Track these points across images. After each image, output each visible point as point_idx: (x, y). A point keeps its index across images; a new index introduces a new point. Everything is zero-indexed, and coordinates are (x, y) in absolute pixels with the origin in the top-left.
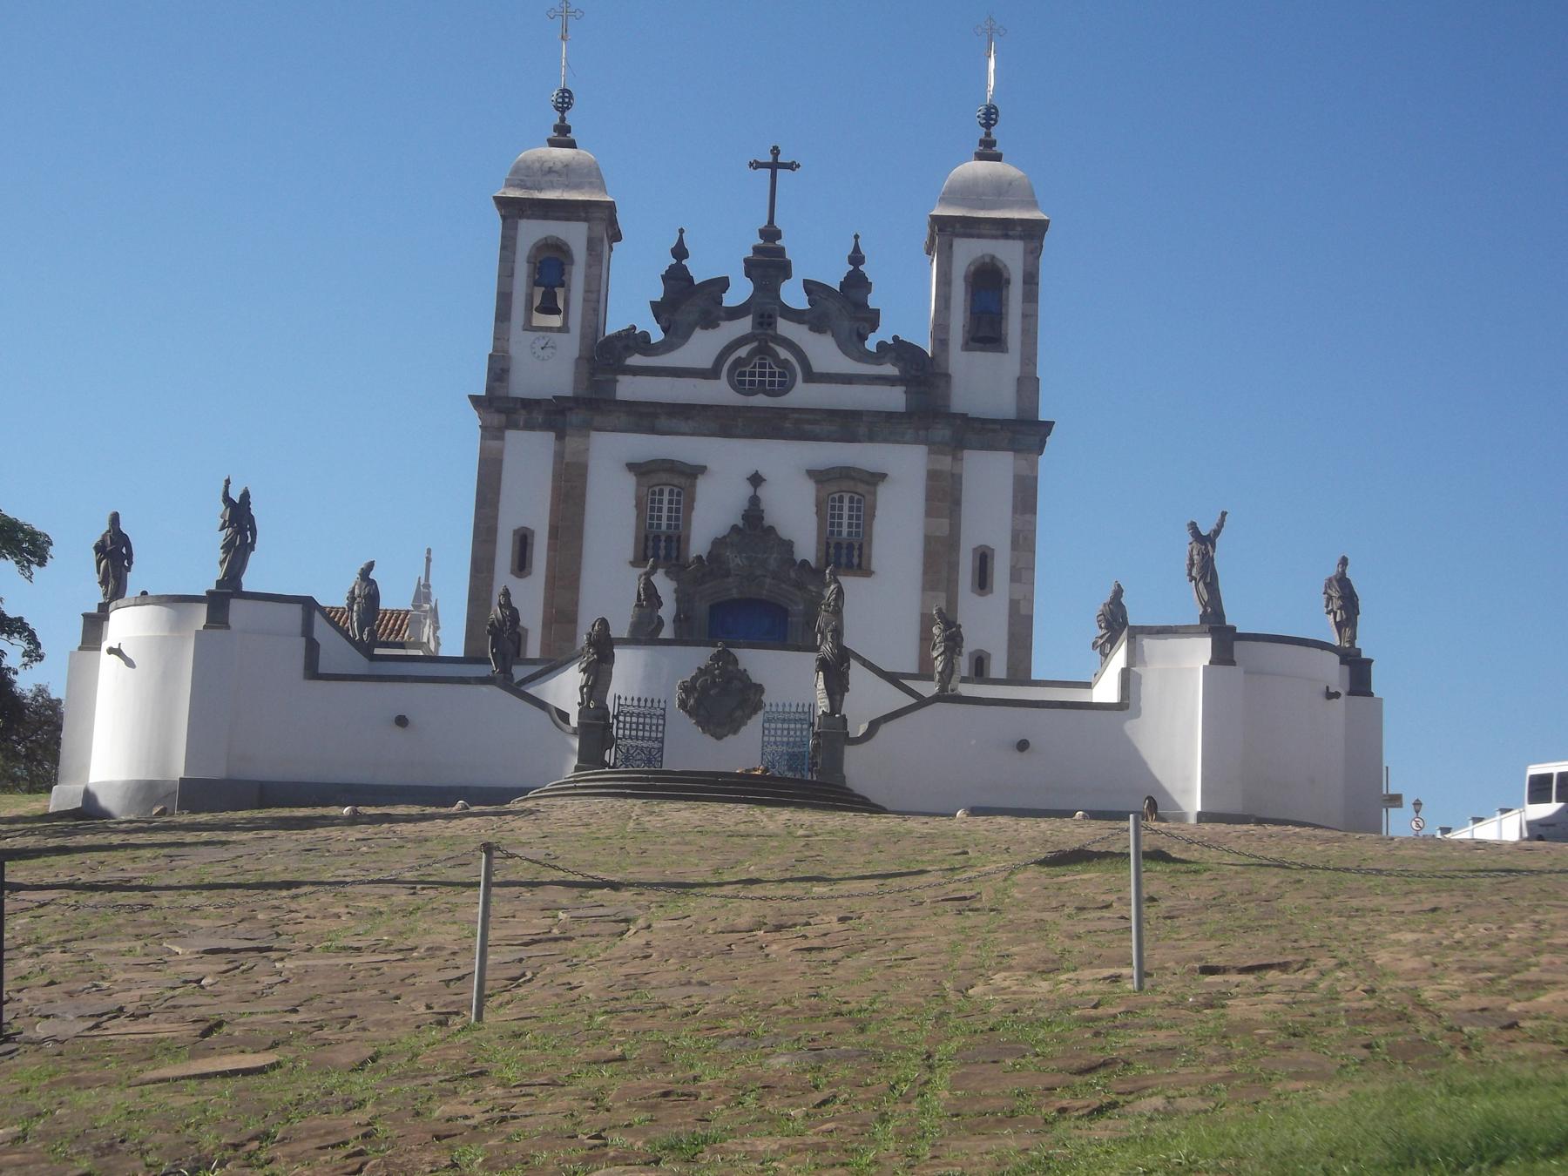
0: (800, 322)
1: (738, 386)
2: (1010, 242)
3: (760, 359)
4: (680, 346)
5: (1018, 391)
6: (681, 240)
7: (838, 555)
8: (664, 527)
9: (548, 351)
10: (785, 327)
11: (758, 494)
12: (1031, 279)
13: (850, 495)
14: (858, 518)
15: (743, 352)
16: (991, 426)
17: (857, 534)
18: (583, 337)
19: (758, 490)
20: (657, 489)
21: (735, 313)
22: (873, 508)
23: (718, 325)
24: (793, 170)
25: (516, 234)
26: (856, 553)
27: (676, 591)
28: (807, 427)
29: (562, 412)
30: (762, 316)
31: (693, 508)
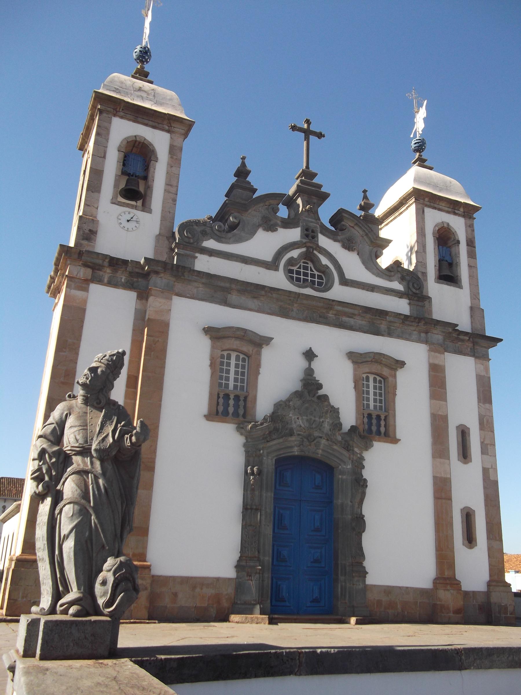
0: (335, 240)
1: (291, 279)
2: (456, 217)
3: (304, 263)
4: (247, 240)
5: (471, 316)
6: (243, 164)
7: (370, 424)
8: (231, 387)
9: (132, 225)
10: (324, 241)
11: (312, 367)
12: (471, 243)
13: (373, 376)
14: (380, 395)
15: (295, 253)
16: (461, 337)
17: (381, 407)
18: (163, 218)
19: (312, 363)
20: (225, 353)
21: (287, 224)
22: (395, 387)
23: (276, 230)
24: (319, 138)
25: (110, 127)
26: (383, 423)
27: (245, 445)
28: (345, 319)
29: (146, 276)
30: (307, 230)
31: (259, 373)
